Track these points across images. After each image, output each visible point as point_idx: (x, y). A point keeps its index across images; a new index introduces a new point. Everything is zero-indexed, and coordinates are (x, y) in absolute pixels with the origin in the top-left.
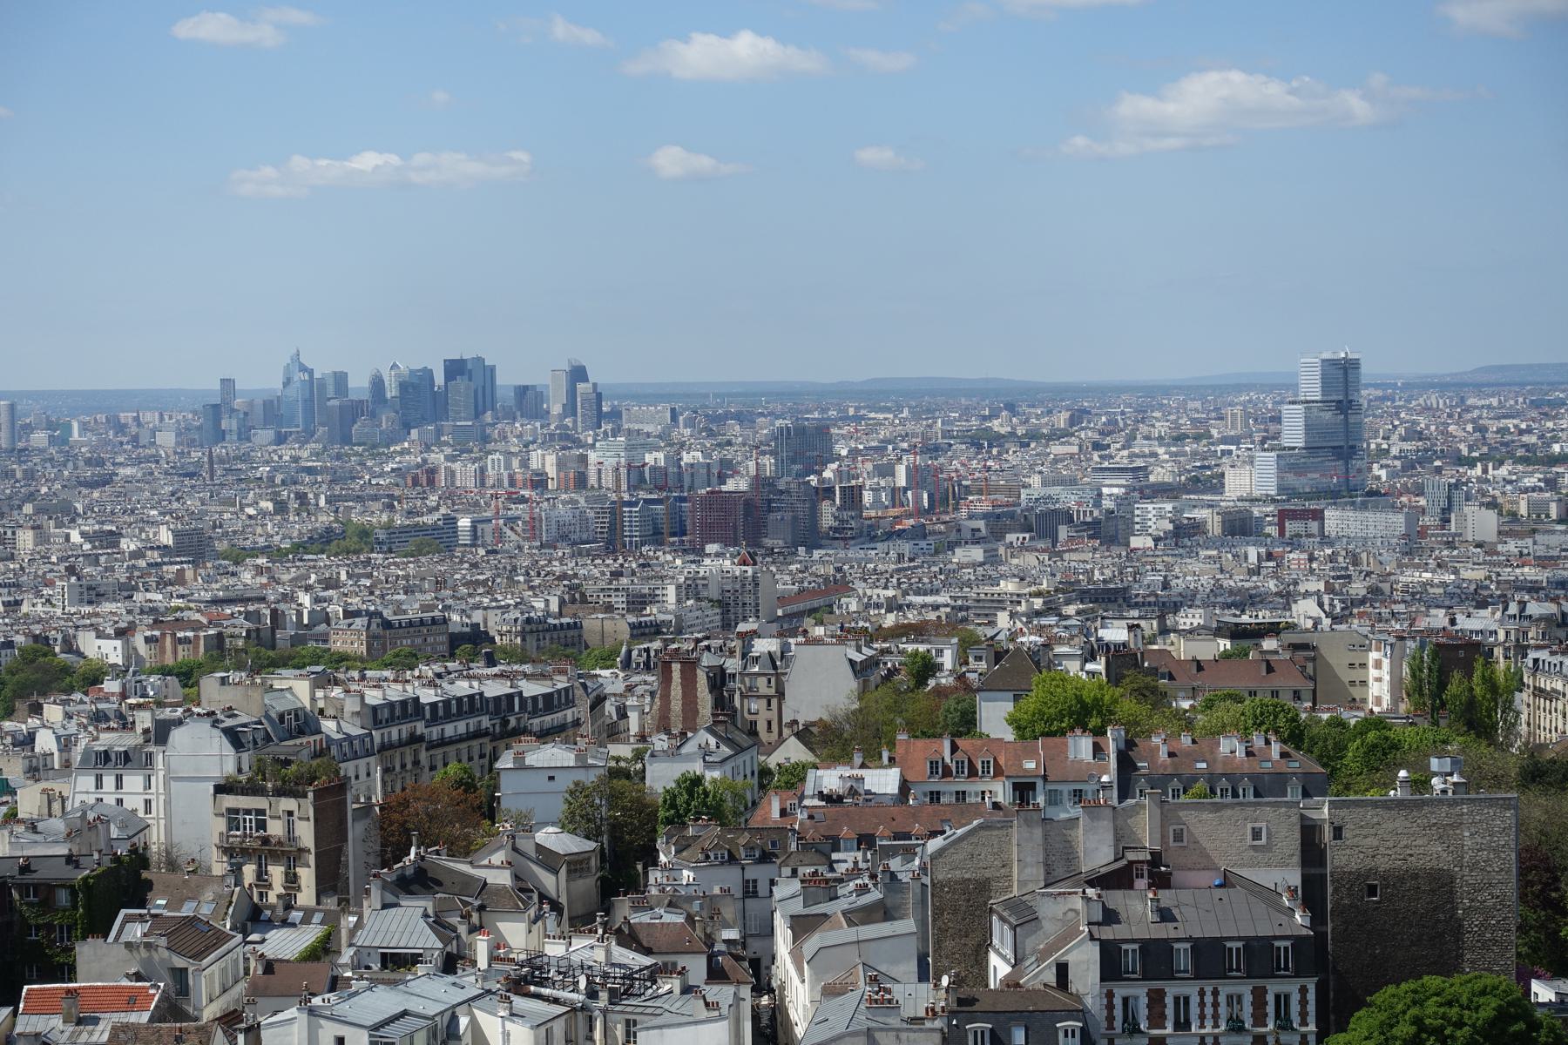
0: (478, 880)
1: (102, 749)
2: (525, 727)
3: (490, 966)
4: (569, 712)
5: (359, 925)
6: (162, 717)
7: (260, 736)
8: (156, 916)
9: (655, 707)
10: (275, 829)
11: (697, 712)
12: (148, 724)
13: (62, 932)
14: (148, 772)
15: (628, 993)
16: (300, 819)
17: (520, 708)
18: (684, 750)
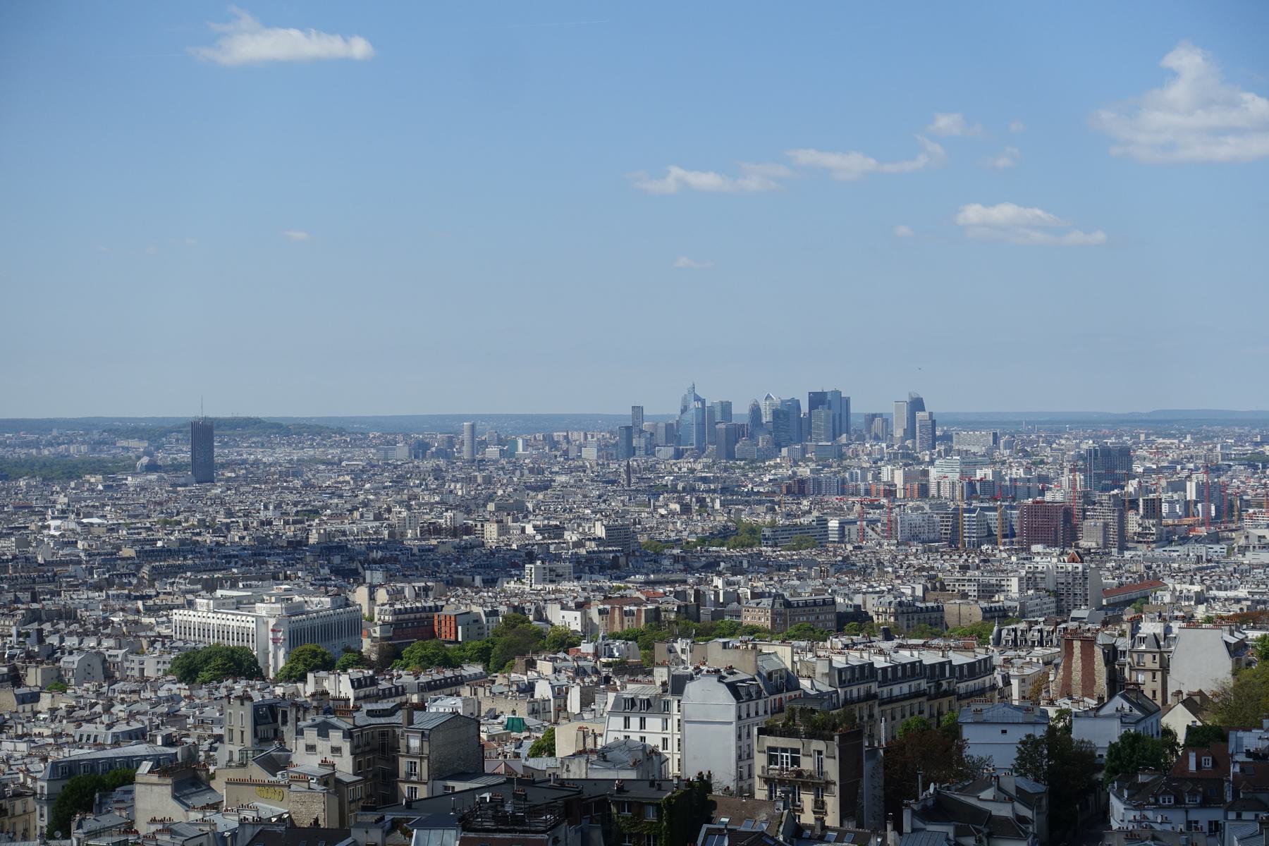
1: (630, 696)
2: (954, 690)
4: (987, 679)
6: (676, 673)
9: (1058, 677)
10: (807, 764)
11: (1094, 682)
13: (649, 840)
14: (666, 716)
16: (827, 757)
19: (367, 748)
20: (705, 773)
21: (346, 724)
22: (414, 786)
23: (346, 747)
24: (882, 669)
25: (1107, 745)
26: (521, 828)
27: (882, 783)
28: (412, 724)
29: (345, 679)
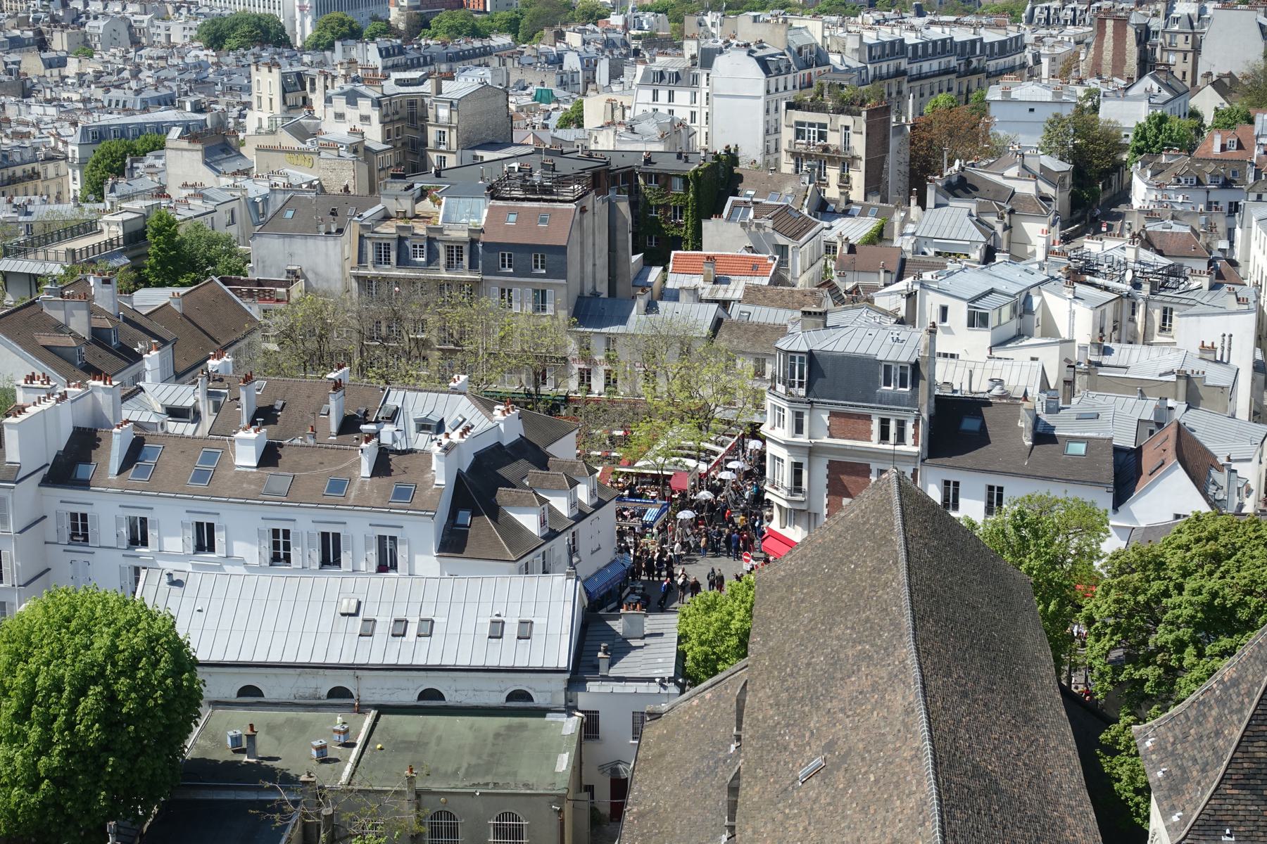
0: (1008, 189)
1: (659, 69)
2: (984, 67)
3: (1046, 259)
4: (1017, 57)
5: (905, 221)
6: (706, 46)
7: (783, 65)
8: (757, 203)
10: (834, 140)
11: (1124, 62)
12: (694, 51)
13: (675, 211)
14: (695, 90)
15: (1163, 287)
17: (981, 52)
18: (1131, 93)
19: (396, 117)
20: (732, 147)
21: (374, 93)
22: (443, 155)
23: (375, 115)
24: (913, 45)
25: (1134, 125)
26: (549, 197)
27: (908, 159)
28: (441, 93)
29: (373, 48)
